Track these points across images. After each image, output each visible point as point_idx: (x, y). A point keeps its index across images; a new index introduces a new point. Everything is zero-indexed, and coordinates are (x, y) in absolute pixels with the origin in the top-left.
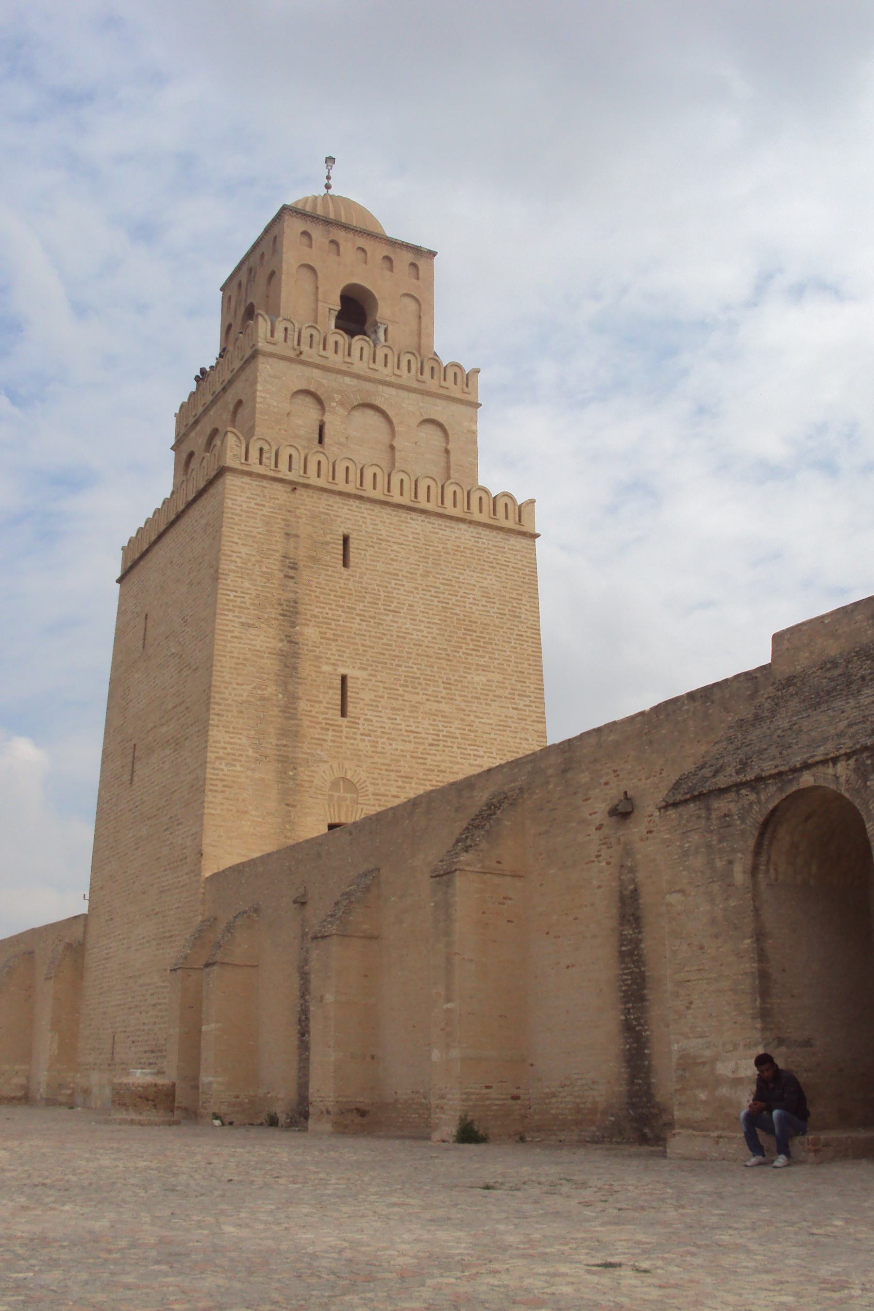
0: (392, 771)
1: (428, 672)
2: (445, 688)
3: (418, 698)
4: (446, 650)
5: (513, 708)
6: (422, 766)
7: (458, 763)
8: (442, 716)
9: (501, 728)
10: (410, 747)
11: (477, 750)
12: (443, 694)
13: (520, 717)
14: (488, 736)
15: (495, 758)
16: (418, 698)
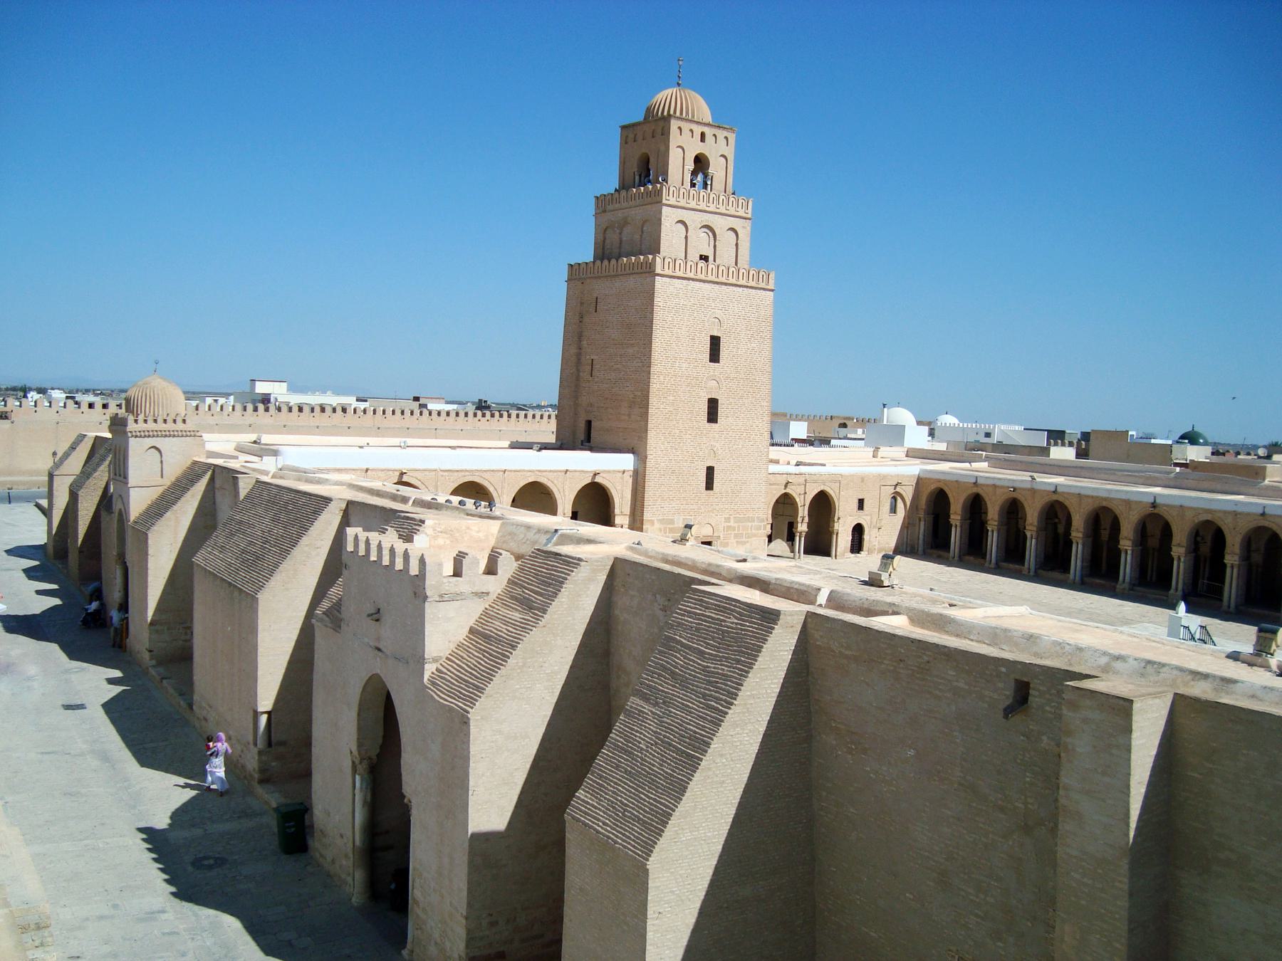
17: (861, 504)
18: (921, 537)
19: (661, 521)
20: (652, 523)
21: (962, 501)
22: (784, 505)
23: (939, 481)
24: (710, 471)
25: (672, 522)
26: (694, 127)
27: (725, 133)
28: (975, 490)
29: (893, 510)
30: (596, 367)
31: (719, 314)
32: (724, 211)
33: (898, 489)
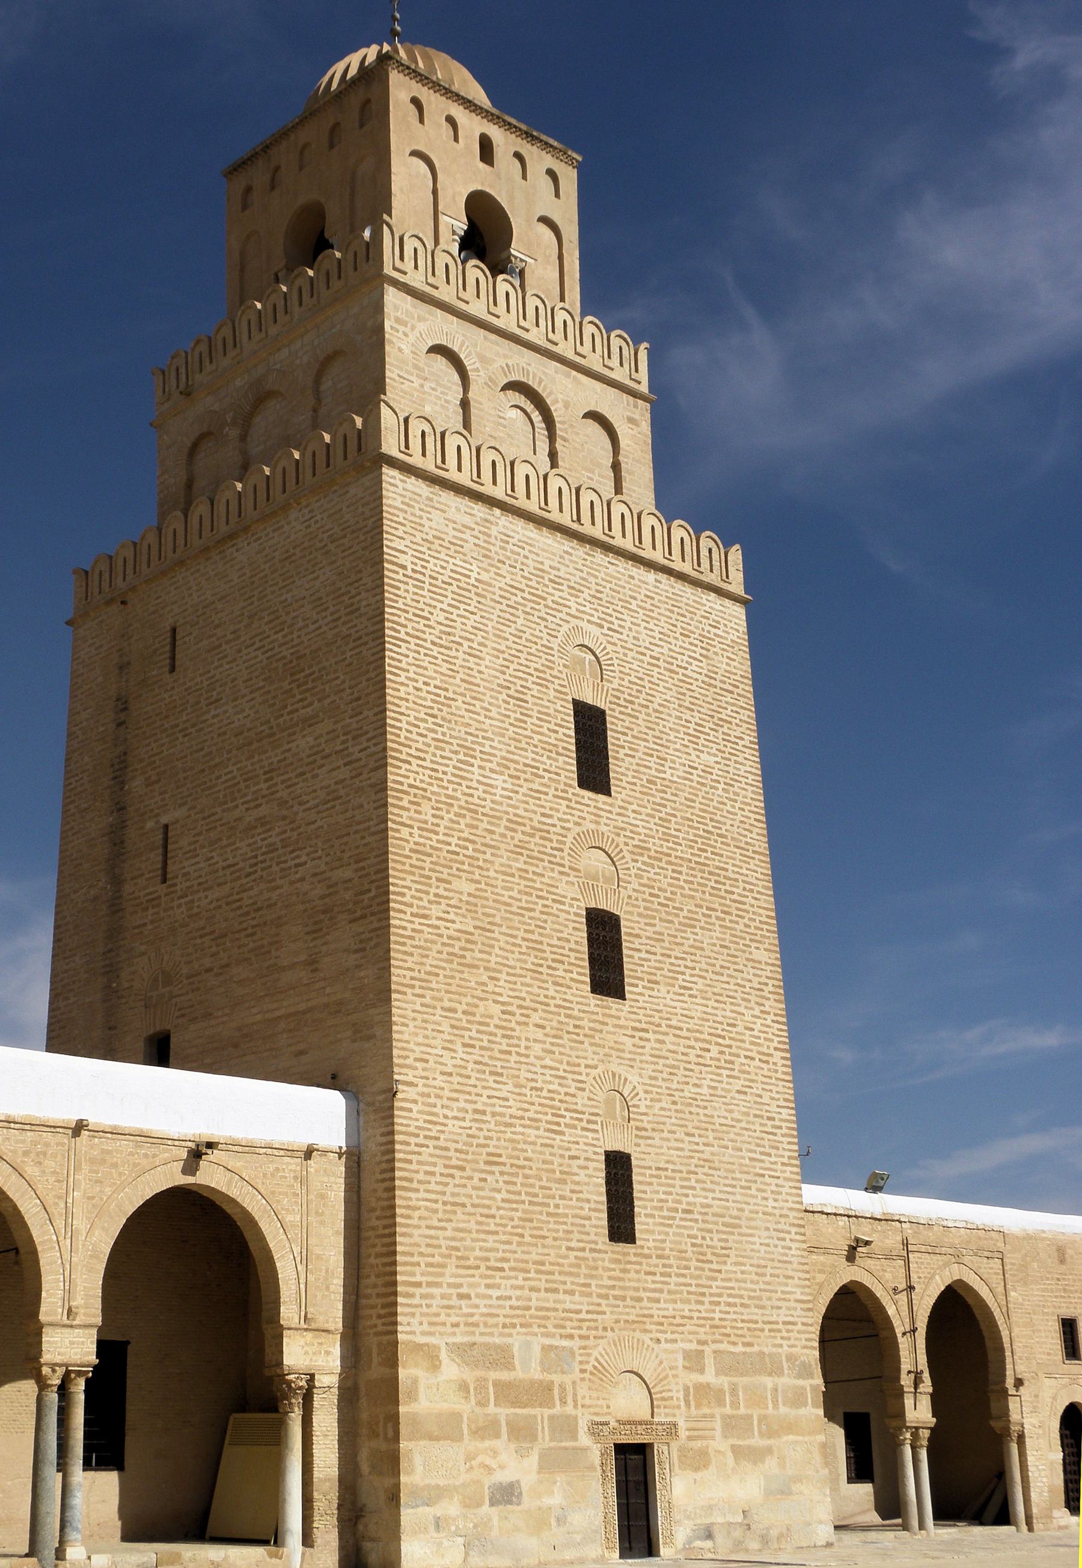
0: (206, 935)
1: (250, 768)
2: (266, 781)
3: (236, 813)
4: (269, 722)
5: (345, 765)
6: (238, 912)
7: (277, 888)
8: (262, 825)
9: (329, 805)
10: (226, 889)
11: (298, 857)
12: (265, 792)
13: (354, 773)
14: (313, 827)
15: (320, 858)
16: (236, 813)
25: (502, 1357)
31: (593, 635)
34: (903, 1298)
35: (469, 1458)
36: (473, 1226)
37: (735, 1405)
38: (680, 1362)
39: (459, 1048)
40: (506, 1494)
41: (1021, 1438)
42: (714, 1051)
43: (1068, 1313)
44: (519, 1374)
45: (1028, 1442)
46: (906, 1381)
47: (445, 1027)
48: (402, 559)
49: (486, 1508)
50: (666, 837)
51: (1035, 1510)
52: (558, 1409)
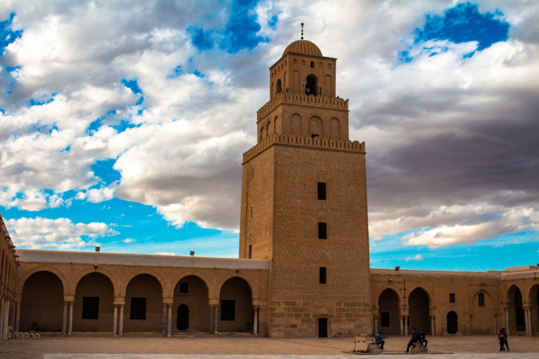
17: (452, 298)
18: (507, 322)
19: (285, 303)
20: (279, 304)
21: (528, 291)
22: (388, 297)
23: (513, 280)
24: (323, 271)
25: (294, 304)
26: (306, 59)
27: (329, 62)
28: (535, 283)
29: (482, 303)
30: (254, 211)
32: (328, 107)
33: (484, 288)
34: (403, 291)
35: (286, 320)
36: (288, 282)
37: (348, 311)
38: (335, 304)
39: (287, 252)
40: (294, 326)
41: (434, 318)
42: (349, 247)
43: (452, 292)
44: (297, 306)
45: (436, 319)
46: (401, 307)
47: (284, 248)
48: (278, 163)
49: (289, 328)
50: (340, 206)
51: (436, 332)
52: (306, 312)
